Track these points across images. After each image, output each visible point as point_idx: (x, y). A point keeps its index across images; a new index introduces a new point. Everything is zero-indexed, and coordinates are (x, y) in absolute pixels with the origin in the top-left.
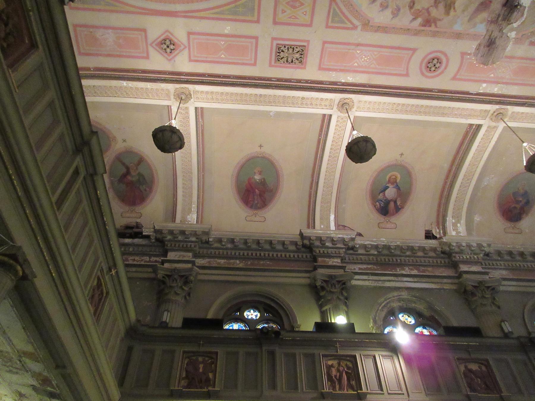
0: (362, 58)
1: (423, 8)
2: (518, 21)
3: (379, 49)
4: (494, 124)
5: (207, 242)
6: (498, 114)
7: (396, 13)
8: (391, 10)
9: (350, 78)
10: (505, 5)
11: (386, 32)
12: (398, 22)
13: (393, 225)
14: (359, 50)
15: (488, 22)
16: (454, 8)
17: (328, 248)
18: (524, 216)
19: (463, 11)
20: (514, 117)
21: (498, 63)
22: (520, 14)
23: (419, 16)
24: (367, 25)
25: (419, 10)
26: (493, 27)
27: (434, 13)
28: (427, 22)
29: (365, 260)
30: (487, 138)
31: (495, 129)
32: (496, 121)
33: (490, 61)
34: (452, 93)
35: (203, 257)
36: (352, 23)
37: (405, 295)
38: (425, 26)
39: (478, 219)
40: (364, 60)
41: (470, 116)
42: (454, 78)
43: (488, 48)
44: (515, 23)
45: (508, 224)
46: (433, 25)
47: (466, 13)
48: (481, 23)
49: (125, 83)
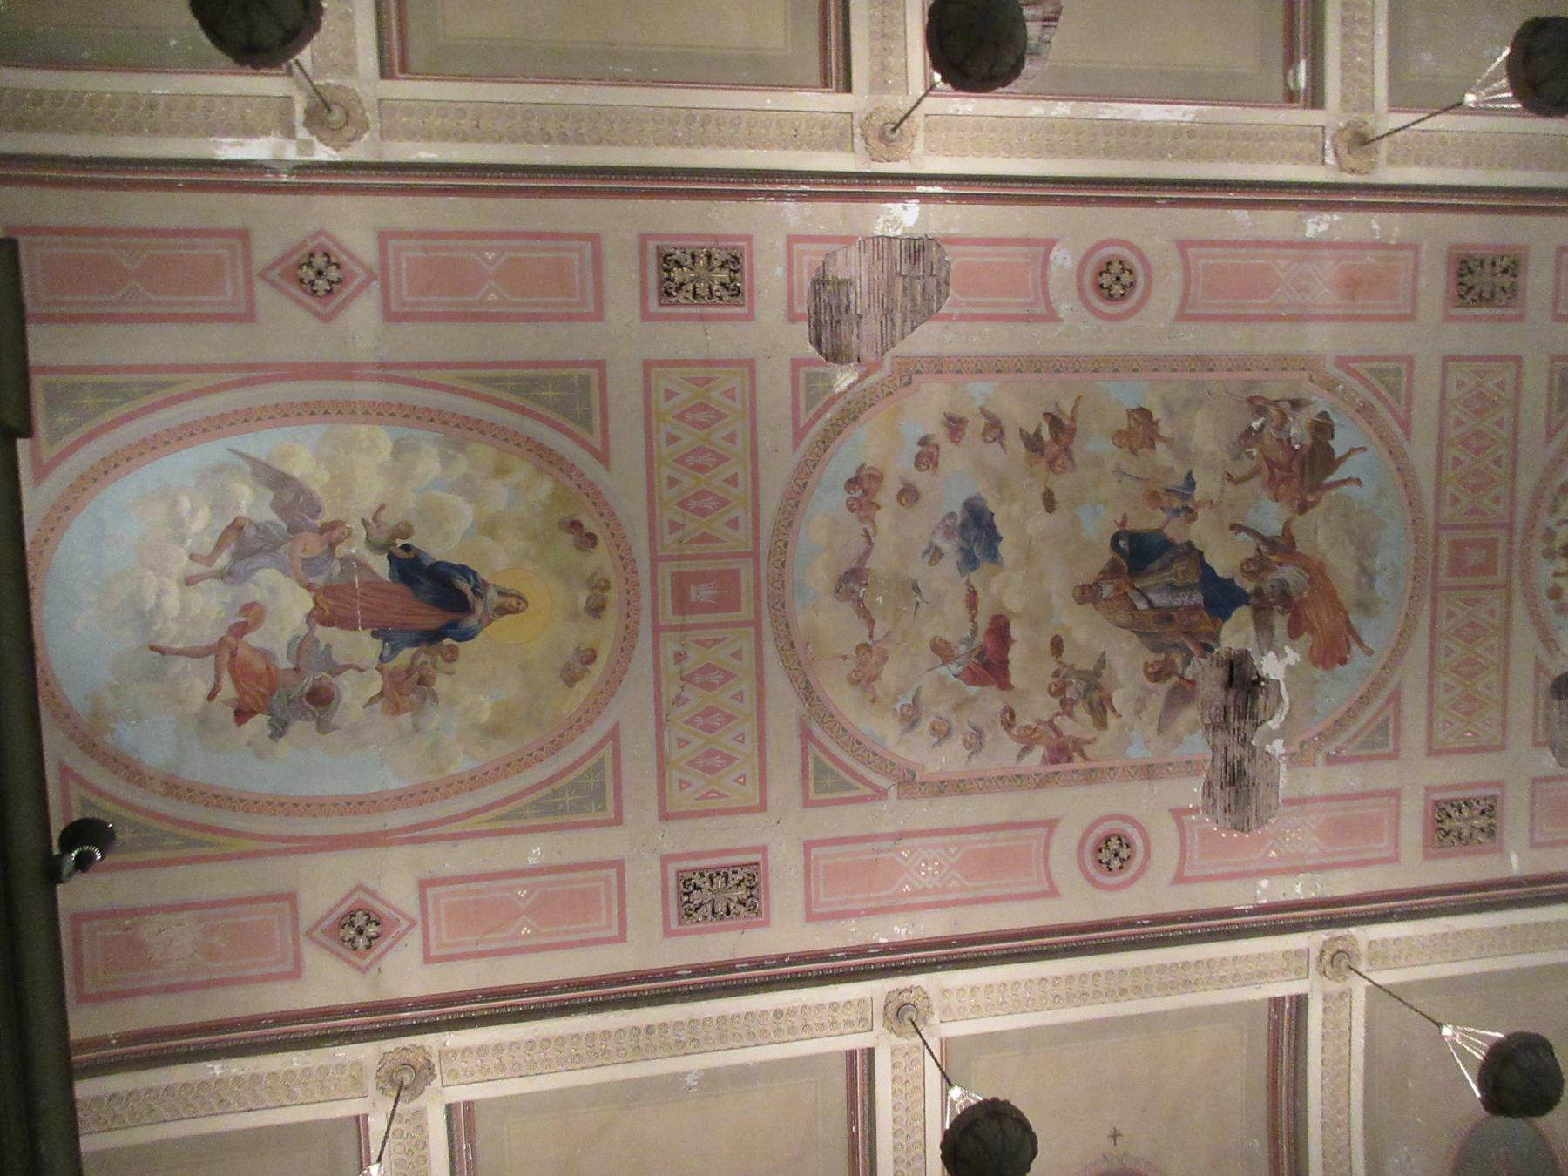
0: (918, 869)
1: (1039, 722)
2: (1277, 716)
3: (955, 838)
4: (1334, 987)
6: (1333, 956)
7: (976, 741)
8: (961, 737)
9: (900, 930)
10: (1229, 684)
12: (984, 764)
14: (906, 849)
15: (1206, 728)
16: (1114, 710)
19: (1138, 713)
20: (1382, 955)
21: (1272, 821)
22: (1272, 698)
23: (1037, 741)
24: (909, 783)
25: (1027, 727)
26: (1222, 738)
27: (1069, 728)
28: (1061, 752)
30: (1337, 1033)
31: (1347, 1000)
32: (1338, 975)
33: (1253, 818)
34: (1190, 920)
38: (1058, 762)
40: (927, 872)
41: (1262, 976)
42: (1179, 879)
43: (1233, 789)
44: (1271, 719)
46: (1075, 755)
47: (1145, 717)
48: (1192, 733)
49: (217, 1068)
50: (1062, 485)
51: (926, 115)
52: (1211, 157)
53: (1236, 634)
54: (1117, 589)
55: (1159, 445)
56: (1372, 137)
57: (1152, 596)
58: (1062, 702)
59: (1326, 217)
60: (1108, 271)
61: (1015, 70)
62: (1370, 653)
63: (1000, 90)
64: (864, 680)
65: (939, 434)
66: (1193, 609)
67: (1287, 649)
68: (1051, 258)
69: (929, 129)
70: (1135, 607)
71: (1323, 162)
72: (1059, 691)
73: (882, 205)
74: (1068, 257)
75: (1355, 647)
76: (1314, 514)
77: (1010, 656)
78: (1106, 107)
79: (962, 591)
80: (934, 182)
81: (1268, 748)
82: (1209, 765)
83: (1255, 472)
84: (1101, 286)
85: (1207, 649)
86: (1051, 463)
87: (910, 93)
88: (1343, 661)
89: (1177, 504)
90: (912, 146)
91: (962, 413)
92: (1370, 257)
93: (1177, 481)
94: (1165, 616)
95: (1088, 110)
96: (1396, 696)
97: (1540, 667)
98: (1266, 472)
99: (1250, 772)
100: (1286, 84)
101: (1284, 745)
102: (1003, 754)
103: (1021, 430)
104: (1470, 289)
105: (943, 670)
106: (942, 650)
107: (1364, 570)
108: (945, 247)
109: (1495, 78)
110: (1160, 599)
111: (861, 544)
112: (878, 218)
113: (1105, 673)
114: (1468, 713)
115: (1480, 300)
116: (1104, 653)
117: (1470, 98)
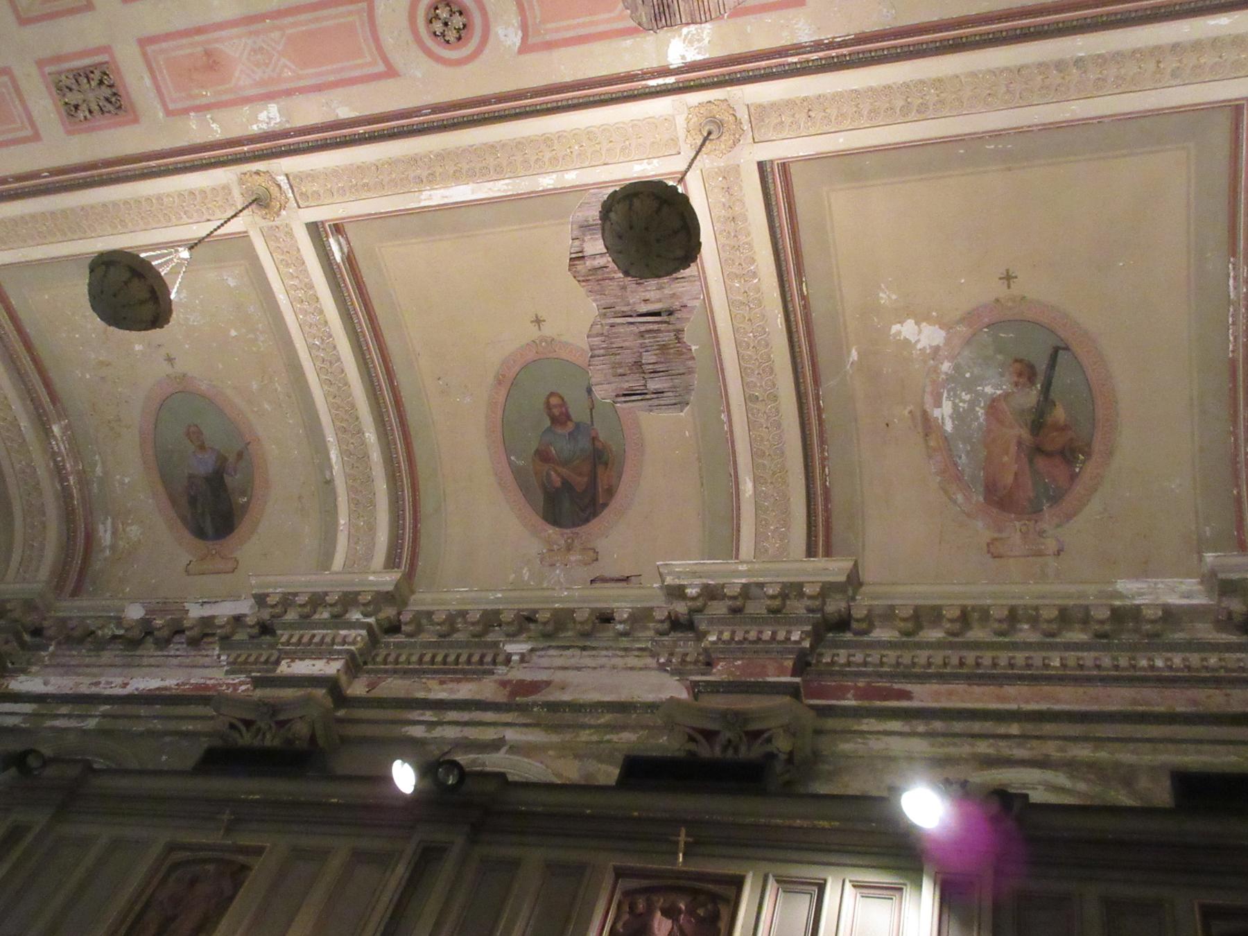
51: (679, 153)
52: (392, 163)
56: (254, 206)
59: (264, 126)
60: (458, 30)
61: (608, 208)
63: (618, 189)
68: (520, 34)
69: (674, 141)
71: (287, 175)
73: (707, 56)
74: (503, 38)
78: (504, 191)
80: (658, 89)
84: (461, 13)
87: (699, 172)
90: (688, 121)
92: (208, 95)
95: (523, 185)
100: (348, 243)
104: (101, 82)
108: (632, 24)
109: (174, 272)
112: (709, 42)
115: (87, 73)
117: (185, 254)
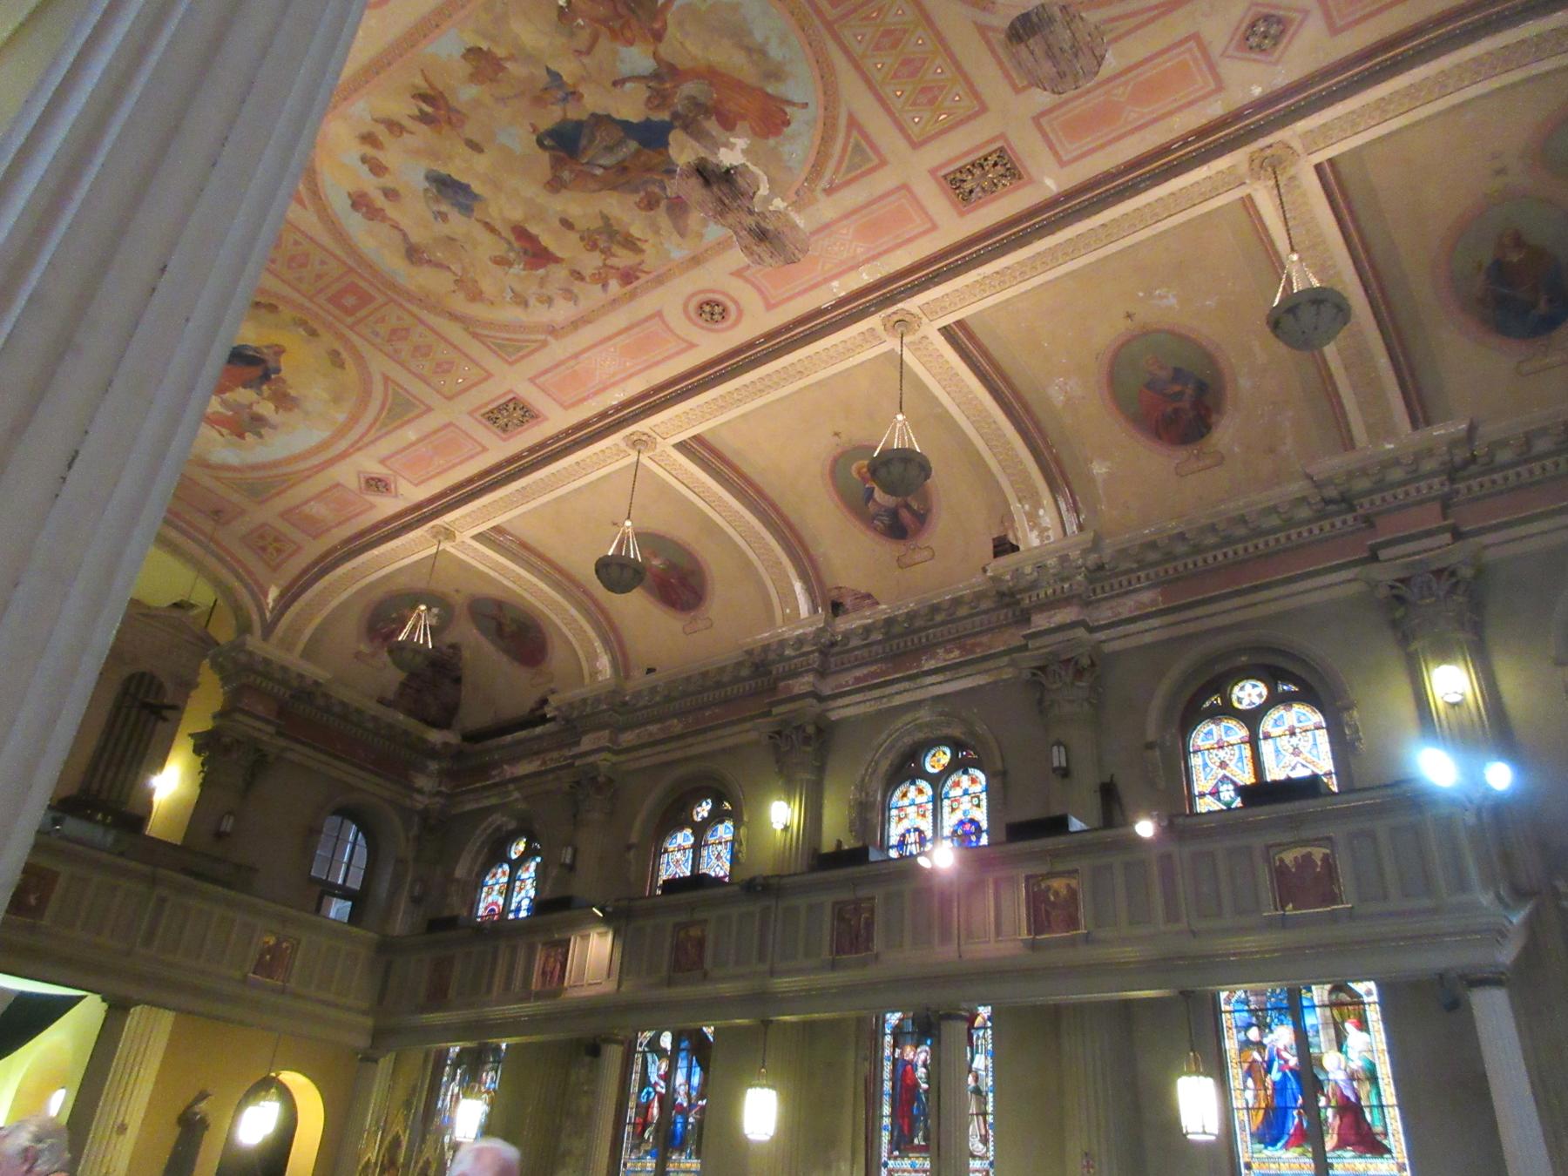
1: (598, 268)
5: (625, 704)
9: (616, 396)
10: (707, 183)
11: (590, 322)
12: (585, 304)
13: (926, 553)
16: (639, 239)
17: (790, 658)
18: (1214, 418)
24: (554, 331)
26: (731, 219)
28: (628, 277)
29: (863, 658)
35: (626, 728)
36: (536, 341)
37: (924, 715)
39: (1104, 470)
44: (758, 189)
45: (1182, 453)
49: (375, 552)
50: (470, 130)
53: (683, 151)
54: (571, 171)
55: (508, 65)
57: (602, 162)
58: (602, 252)
62: (805, 105)
64: (476, 296)
65: (369, 150)
66: (637, 154)
67: (732, 140)
70: (595, 175)
72: (593, 246)
75: (788, 109)
76: (672, 30)
77: (543, 244)
79: (479, 226)
81: (771, 208)
82: (735, 238)
83: (595, 39)
85: (670, 172)
86: (449, 121)
88: (787, 123)
89: (560, 94)
91: (365, 129)
93: (544, 78)
94: (622, 168)
96: (853, 123)
97: (983, 30)
98: (603, 29)
99: (770, 227)
101: (783, 200)
102: (592, 295)
103: (410, 116)
105: (512, 270)
106: (501, 261)
107: (749, 50)
110: (607, 161)
111: (395, 234)
113: (612, 221)
114: (931, 102)
116: (601, 212)
